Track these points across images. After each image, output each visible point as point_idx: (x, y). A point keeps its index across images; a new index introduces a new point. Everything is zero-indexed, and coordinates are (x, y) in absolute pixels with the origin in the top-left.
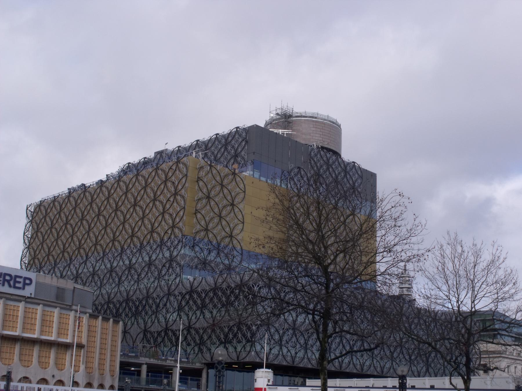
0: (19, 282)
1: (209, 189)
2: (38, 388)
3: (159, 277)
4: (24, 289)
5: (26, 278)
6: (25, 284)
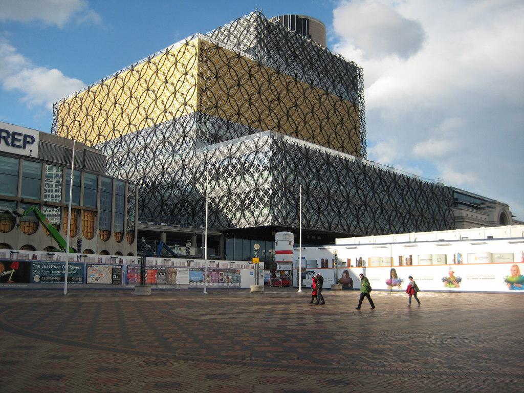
0: (19, 140)
1: (217, 68)
2: (34, 255)
3: (174, 152)
4: (24, 147)
5: (26, 136)
6: (25, 143)
